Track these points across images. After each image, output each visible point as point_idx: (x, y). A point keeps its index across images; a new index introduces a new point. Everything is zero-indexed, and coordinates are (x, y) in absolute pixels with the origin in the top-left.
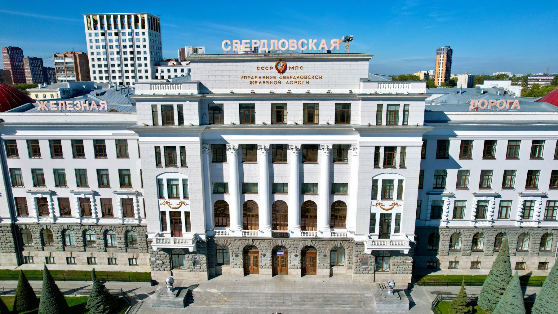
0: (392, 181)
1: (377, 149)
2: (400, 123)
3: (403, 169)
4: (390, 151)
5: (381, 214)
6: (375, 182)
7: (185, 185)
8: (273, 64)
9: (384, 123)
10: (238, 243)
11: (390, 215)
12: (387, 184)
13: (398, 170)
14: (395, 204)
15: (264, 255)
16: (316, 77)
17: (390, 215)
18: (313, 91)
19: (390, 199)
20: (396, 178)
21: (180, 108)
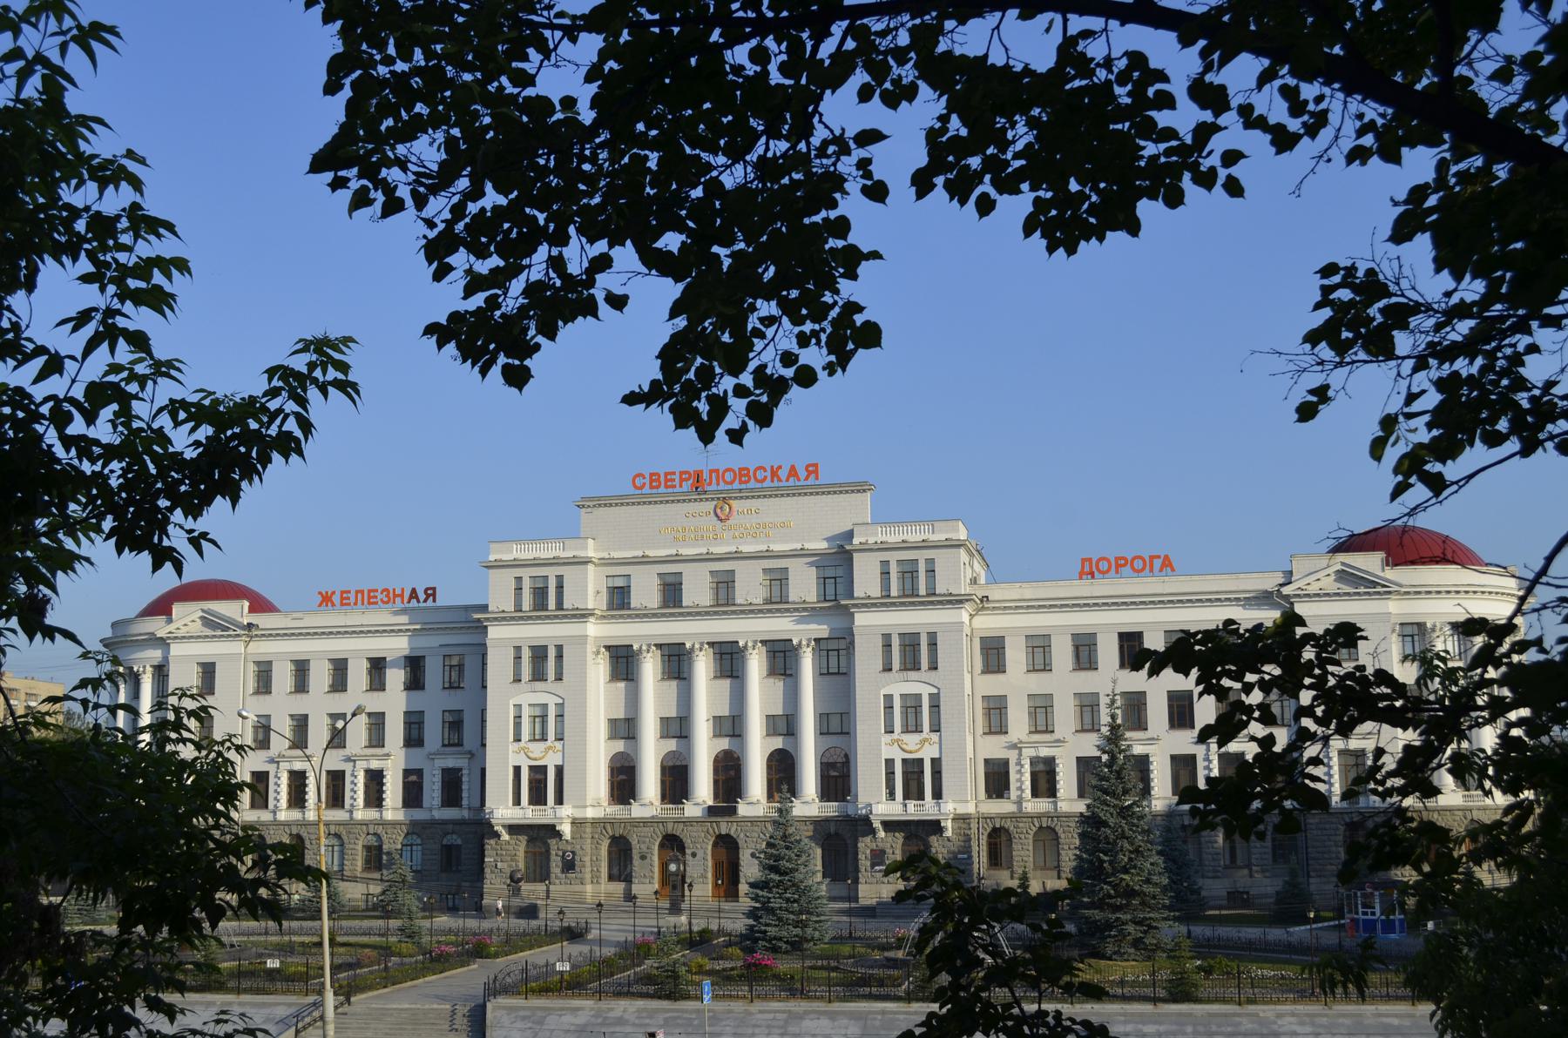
0: (918, 697)
1: (887, 639)
2: (922, 591)
3: (933, 673)
4: (910, 643)
5: (904, 761)
6: (889, 698)
7: (560, 716)
8: (710, 506)
9: (894, 592)
10: (648, 830)
11: (921, 761)
12: (912, 705)
13: (924, 674)
14: (925, 740)
15: (694, 855)
16: (784, 525)
17: (921, 761)
18: (777, 547)
19: (918, 730)
20: (925, 691)
21: (560, 578)
